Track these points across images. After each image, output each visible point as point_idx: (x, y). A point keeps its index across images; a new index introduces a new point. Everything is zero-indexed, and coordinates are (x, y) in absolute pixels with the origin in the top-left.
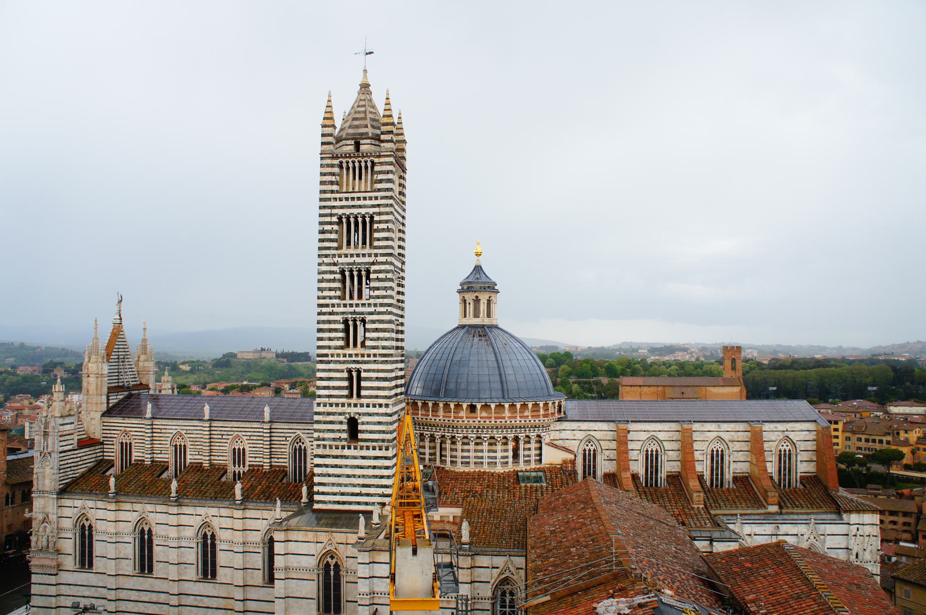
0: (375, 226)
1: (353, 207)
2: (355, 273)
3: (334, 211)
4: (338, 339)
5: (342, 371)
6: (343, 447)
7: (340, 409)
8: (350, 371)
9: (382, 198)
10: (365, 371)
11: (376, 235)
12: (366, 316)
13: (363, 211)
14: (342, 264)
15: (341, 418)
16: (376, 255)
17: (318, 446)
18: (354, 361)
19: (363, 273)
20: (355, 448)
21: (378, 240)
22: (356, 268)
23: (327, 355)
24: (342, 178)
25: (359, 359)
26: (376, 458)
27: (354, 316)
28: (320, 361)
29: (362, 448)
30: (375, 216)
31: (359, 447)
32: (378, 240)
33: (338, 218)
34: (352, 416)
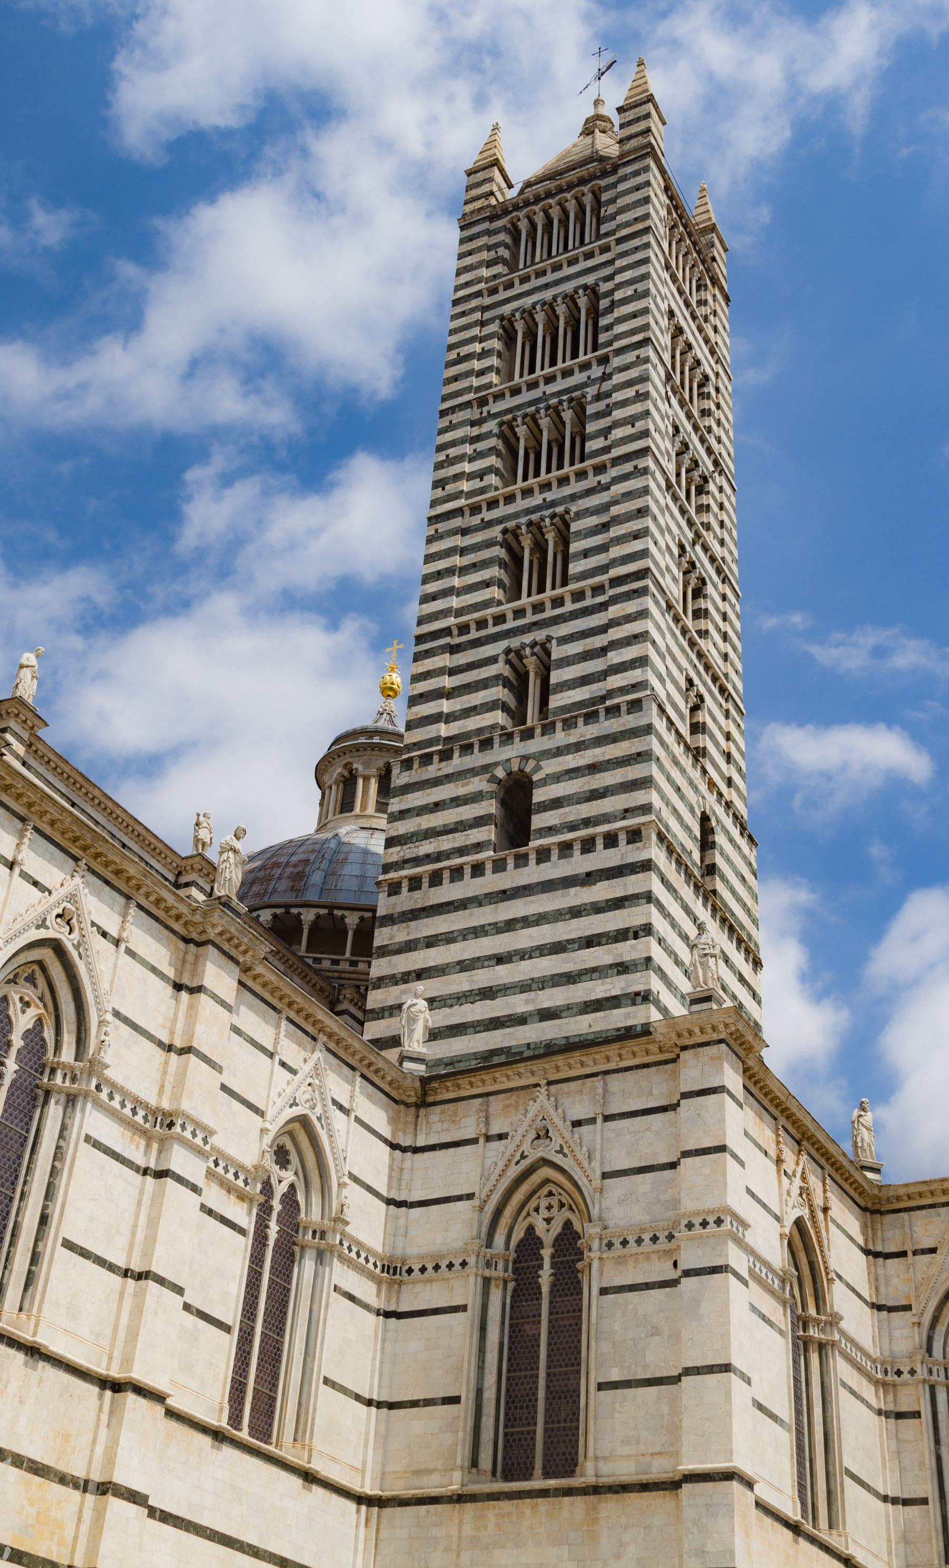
0: (604, 303)
1: (547, 286)
2: (544, 422)
3: (488, 315)
4: (487, 584)
5: (493, 660)
6: (478, 870)
7: (478, 759)
8: (514, 657)
9: (619, 241)
10: (563, 640)
11: (603, 322)
12: (568, 505)
13: (568, 287)
14: (509, 411)
15: (479, 784)
16: (604, 360)
17: (394, 889)
18: (535, 624)
19: (568, 415)
20: (521, 860)
21: (608, 328)
22: (548, 408)
23: (447, 631)
24: (515, 256)
25: (549, 613)
26: (590, 878)
27: (535, 517)
28: (426, 651)
29: (543, 855)
30: (601, 284)
31: (533, 857)
32: (608, 328)
33: (503, 327)
34: (515, 768)
